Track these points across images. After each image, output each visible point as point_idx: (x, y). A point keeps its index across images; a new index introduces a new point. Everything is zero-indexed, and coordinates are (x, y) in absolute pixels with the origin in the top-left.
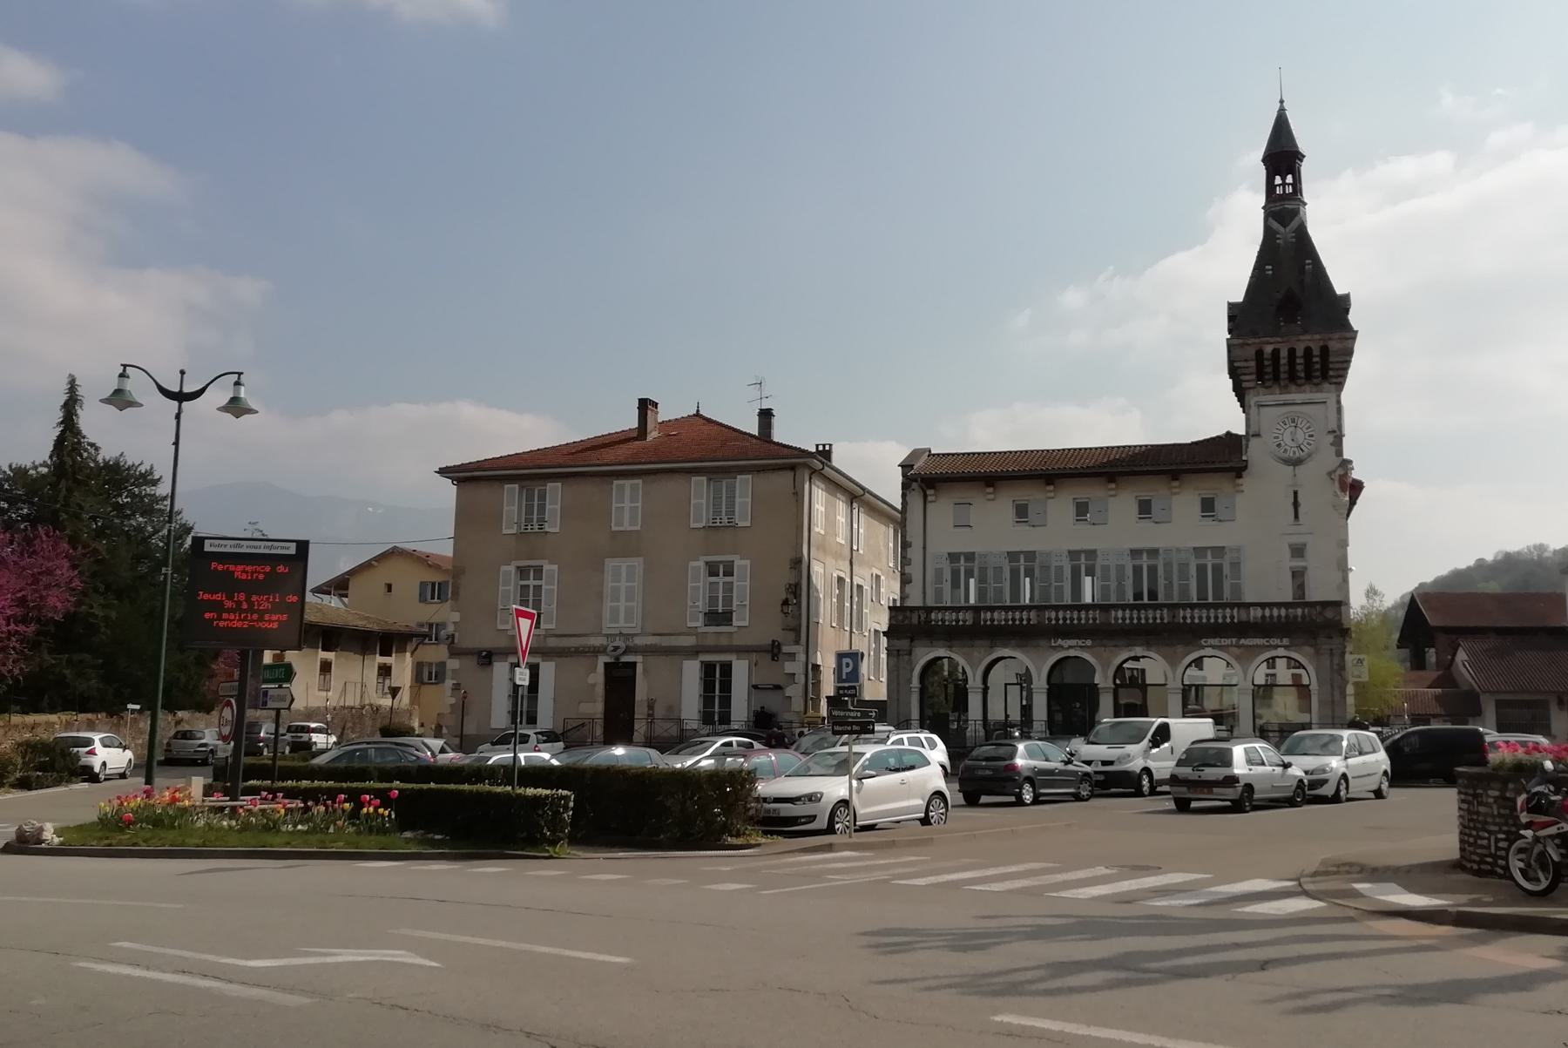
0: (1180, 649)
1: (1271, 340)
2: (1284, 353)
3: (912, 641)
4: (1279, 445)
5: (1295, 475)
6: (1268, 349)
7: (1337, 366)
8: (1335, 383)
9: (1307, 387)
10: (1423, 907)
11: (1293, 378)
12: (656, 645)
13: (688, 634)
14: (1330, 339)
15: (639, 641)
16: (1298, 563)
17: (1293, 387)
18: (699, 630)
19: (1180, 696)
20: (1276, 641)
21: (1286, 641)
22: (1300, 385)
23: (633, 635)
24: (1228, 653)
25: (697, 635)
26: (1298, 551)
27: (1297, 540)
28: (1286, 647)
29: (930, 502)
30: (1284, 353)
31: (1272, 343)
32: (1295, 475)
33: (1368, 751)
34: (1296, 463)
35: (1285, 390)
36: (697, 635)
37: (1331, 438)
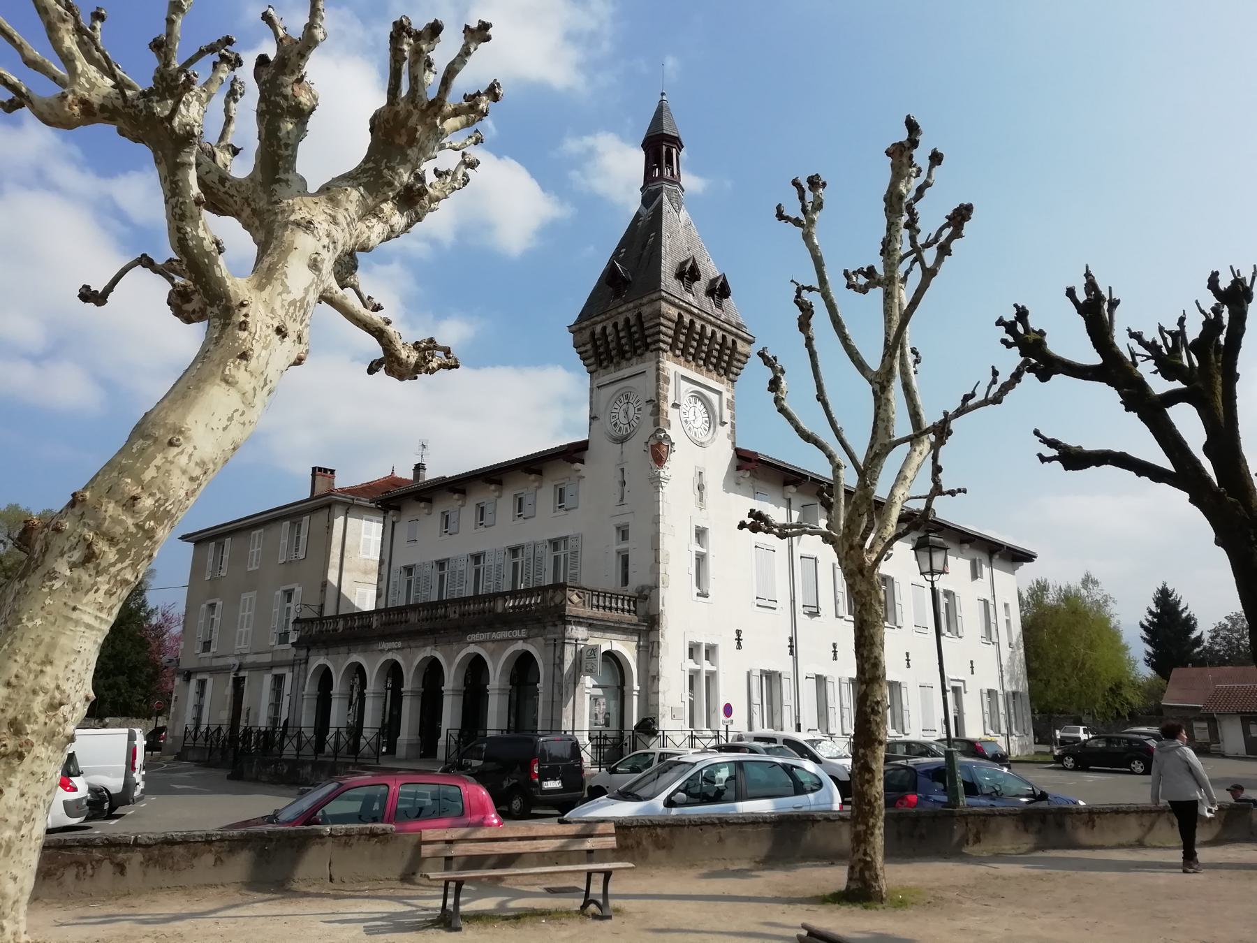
0: (455, 647)
1: (598, 319)
2: (610, 329)
3: (308, 650)
4: (615, 425)
5: (622, 452)
6: (599, 328)
7: (651, 331)
8: (655, 350)
9: (634, 360)
10: (838, 936)
11: (622, 354)
12: (254, 662)
13: (266, 652)
14: (642, 305)
15: (250, 659)
16: (623, 546)
17: (624, 363)
18: (275, 648)
19: (462, 697)
20: (516, 634)
21: (523, 633)
22: (641, 355)
23: (246, 654)
24: (485, 648)
25: (272, 652)
26: (624, 533)
27: (621, 521)
28: (524, 639)
29: (934, 516)
30: (610, 329)
31: (601, 322)
32: (622, 452)
33: (901, 746)
34: (622, 440)
35: (618, 366)
36: (272, 652)
37: (650, 408)
